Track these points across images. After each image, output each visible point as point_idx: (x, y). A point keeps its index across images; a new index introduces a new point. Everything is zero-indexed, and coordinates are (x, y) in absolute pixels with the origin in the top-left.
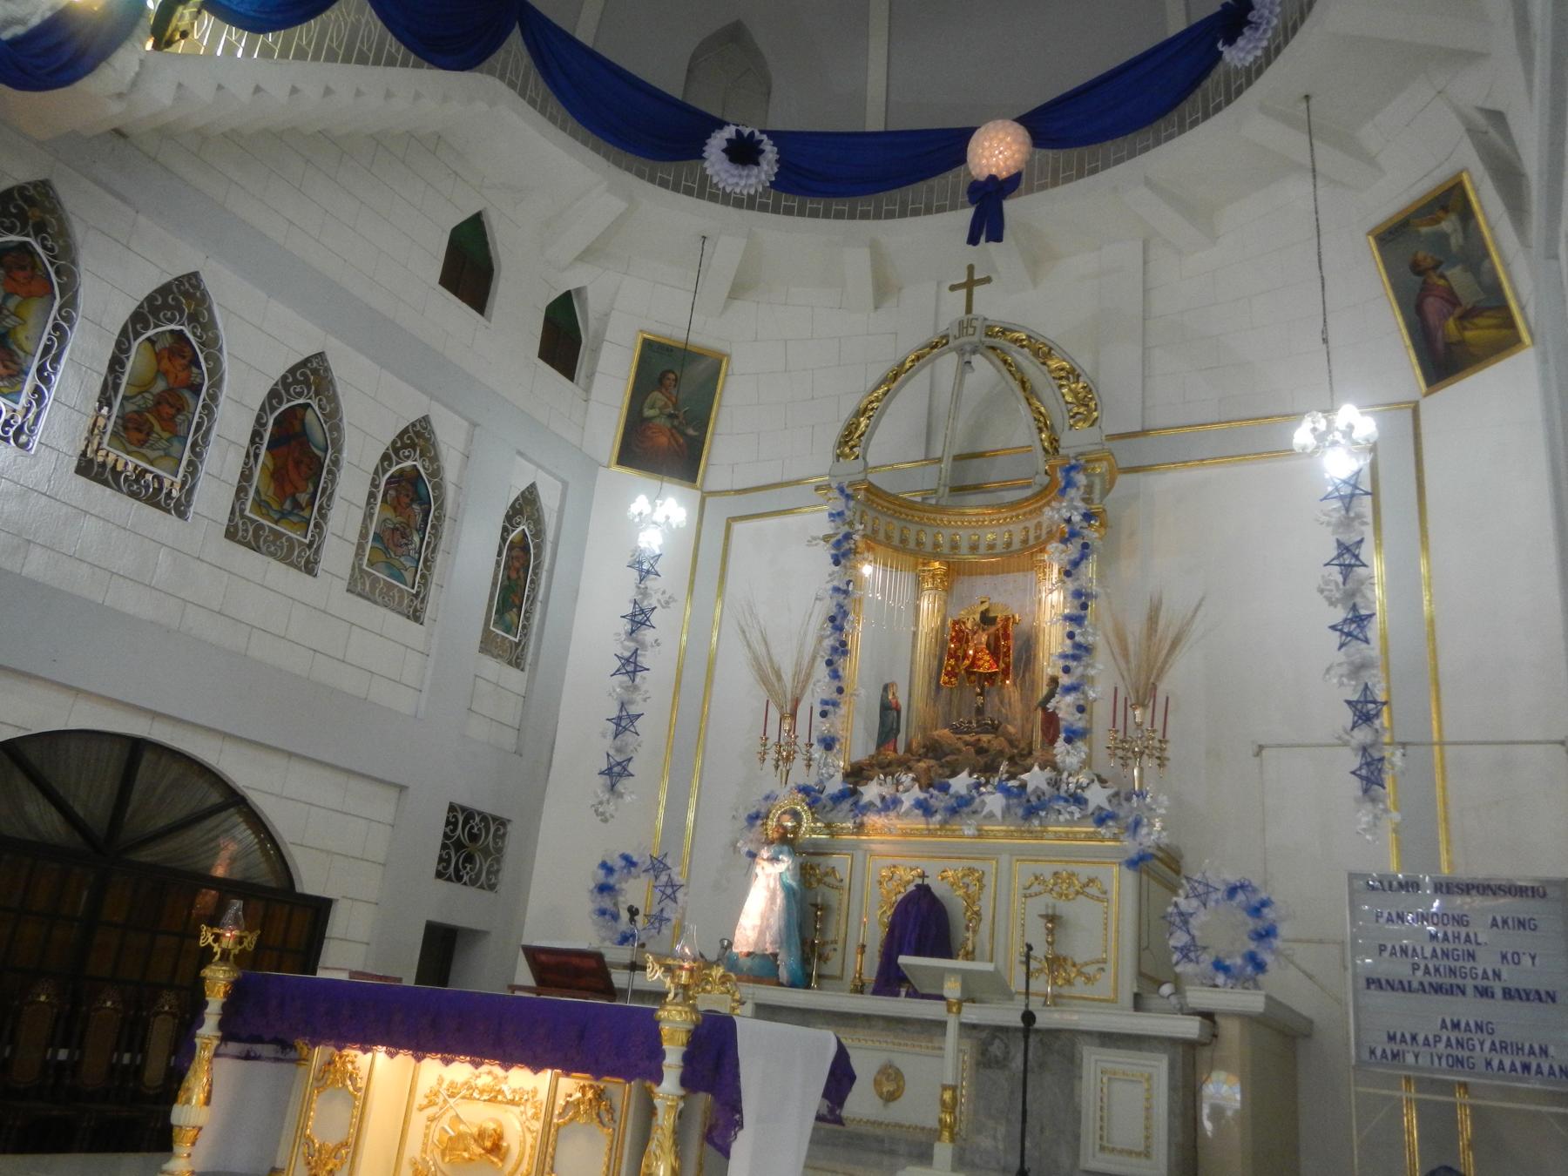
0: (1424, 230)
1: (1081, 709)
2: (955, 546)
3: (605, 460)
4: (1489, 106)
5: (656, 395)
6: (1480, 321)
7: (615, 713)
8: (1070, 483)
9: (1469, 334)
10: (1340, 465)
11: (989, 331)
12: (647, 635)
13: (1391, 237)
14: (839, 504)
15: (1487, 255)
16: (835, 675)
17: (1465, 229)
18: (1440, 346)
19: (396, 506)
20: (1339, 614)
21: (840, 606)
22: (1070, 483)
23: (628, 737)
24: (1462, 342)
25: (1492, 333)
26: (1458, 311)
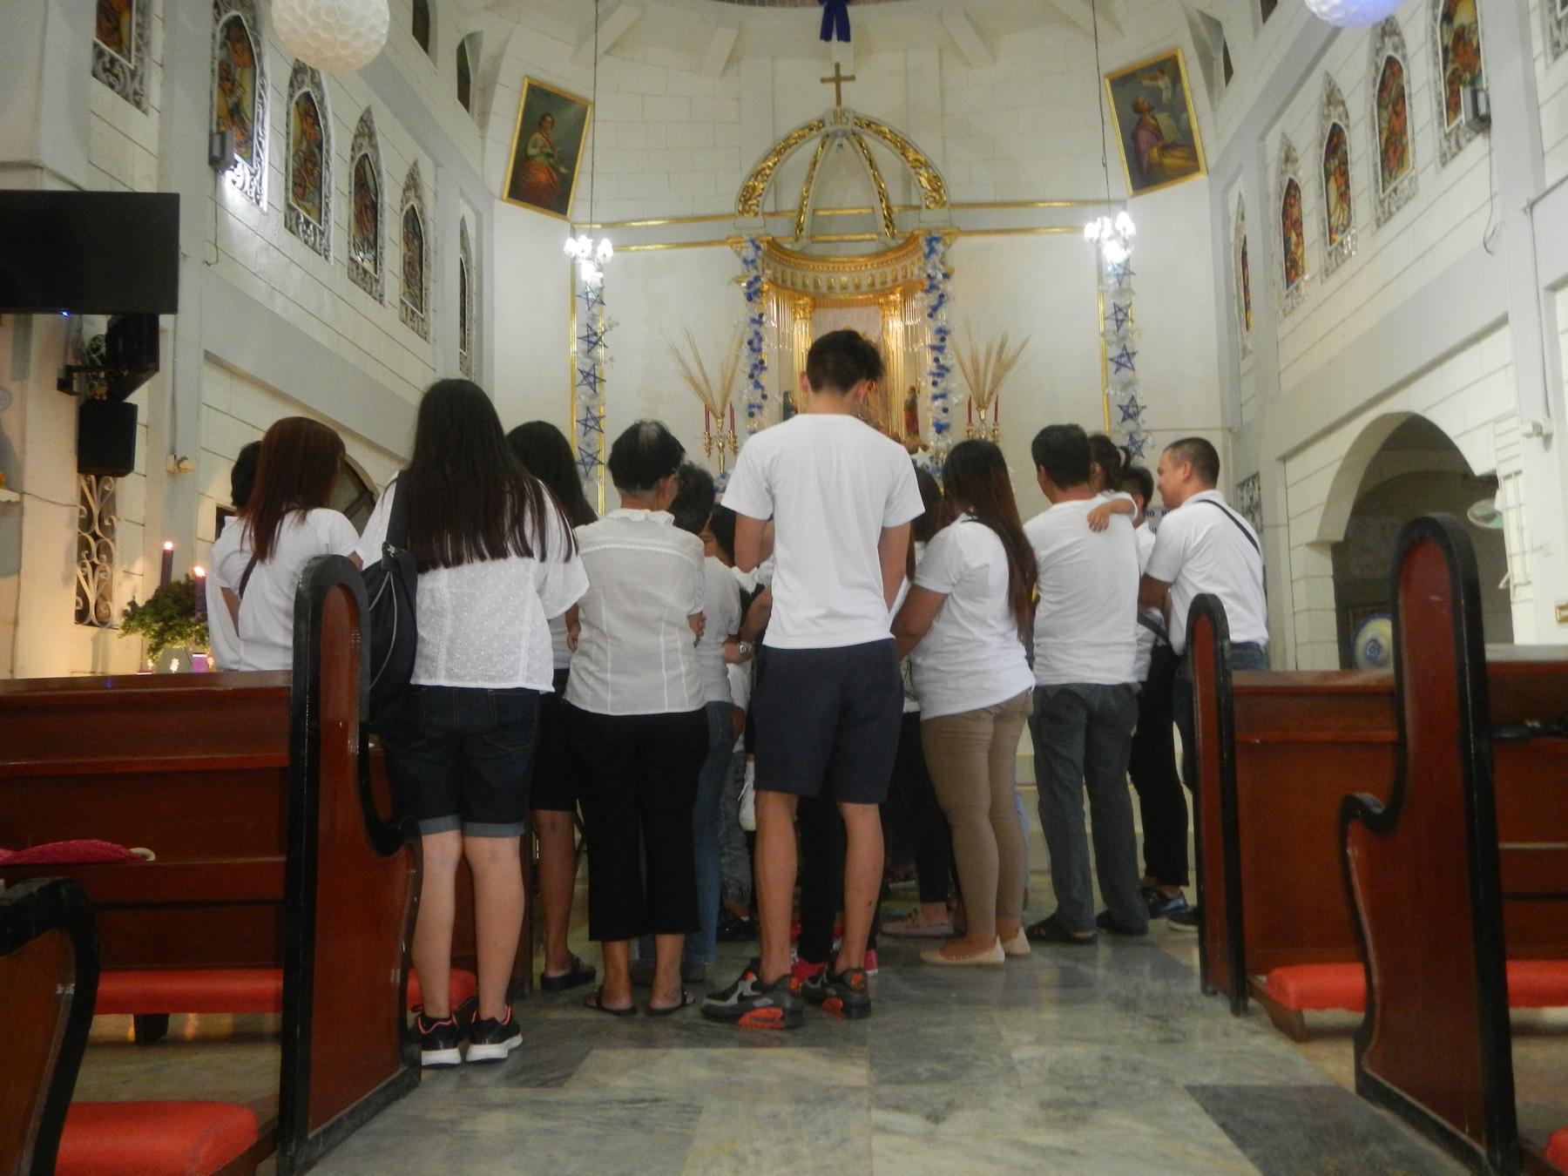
0: (1146, 83)
1: (945, 410)
2: (816, 286)
3: (497, 192)
4: (1209, 12)
5: (538, 136)
6: (1176, 153)
7: (583, 416)
8: (932, 250)
9: (1167, 161)
10: (1115, 255)
11: (858, 121)
12: (600, 352)
13: (1123, 82)
14: (749, 253)
15: (1185, 109)
16: (757, 385)
17: (1174, 91)
18: (1145, 165)
19: (407, 241)
20: (1115, 351)
21: (757, 333)
22: (932, 250)
23: (593, 434)
24: (1161, 164)
25: (1181, 162)
26: (1161, 144)
